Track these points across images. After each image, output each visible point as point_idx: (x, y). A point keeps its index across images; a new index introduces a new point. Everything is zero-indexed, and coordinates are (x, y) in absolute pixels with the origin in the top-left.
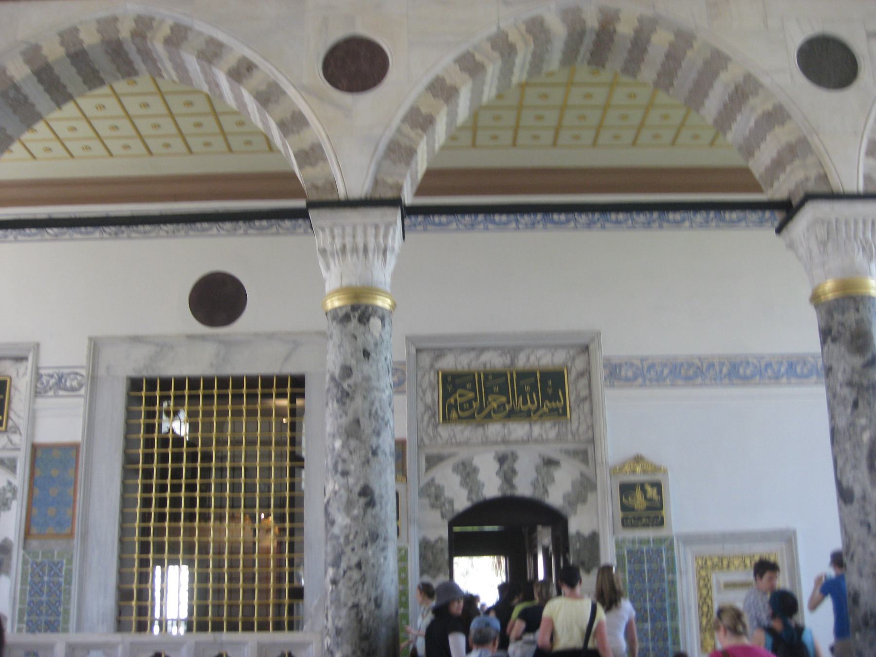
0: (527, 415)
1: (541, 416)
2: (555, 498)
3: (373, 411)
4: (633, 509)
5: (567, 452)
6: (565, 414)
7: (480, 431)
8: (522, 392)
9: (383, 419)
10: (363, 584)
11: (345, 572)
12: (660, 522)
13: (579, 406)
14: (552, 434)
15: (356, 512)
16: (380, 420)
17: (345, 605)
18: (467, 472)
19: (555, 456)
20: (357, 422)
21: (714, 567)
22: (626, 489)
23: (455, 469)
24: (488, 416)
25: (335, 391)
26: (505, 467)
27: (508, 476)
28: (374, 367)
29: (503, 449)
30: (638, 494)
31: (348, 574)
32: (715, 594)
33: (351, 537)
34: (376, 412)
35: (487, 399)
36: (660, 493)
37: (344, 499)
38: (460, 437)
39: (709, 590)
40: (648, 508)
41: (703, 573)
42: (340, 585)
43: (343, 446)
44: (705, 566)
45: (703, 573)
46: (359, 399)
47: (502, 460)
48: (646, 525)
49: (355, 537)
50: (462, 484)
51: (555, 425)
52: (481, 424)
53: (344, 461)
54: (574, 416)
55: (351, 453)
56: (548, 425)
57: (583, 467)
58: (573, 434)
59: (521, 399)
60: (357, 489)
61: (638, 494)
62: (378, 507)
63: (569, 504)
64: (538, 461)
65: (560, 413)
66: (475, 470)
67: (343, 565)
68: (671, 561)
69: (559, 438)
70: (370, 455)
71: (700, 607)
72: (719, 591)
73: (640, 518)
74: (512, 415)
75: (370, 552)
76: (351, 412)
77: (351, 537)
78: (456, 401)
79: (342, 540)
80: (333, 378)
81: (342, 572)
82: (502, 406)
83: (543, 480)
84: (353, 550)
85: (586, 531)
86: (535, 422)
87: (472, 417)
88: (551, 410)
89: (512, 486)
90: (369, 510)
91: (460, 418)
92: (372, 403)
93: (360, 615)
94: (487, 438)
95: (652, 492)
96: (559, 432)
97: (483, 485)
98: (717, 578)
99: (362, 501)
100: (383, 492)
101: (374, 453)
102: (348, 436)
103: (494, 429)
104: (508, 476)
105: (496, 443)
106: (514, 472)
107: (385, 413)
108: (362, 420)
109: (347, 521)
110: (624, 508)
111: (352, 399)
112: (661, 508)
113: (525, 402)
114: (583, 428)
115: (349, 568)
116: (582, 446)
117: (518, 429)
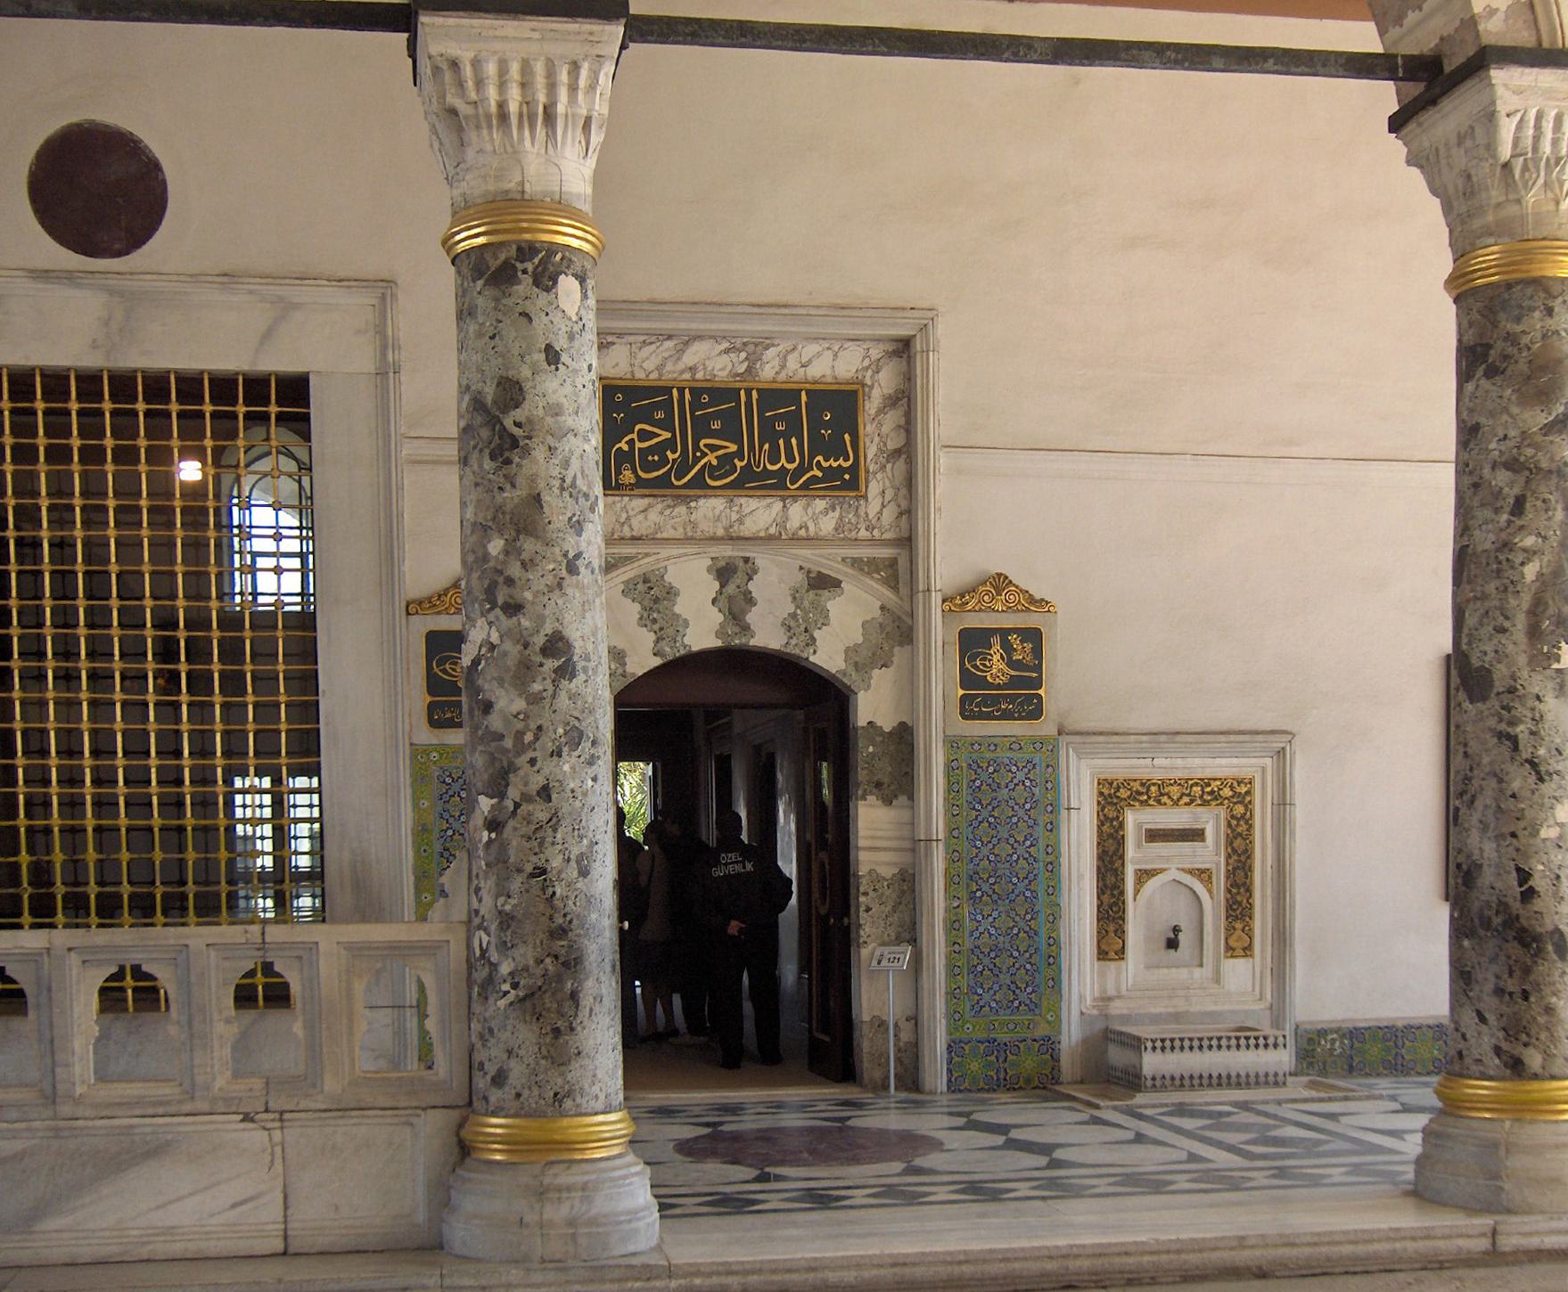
0: (776, 484)
1: (805, 487)
2: (828, 656)
3: (568, 481)
4: (982, 683)
5: (856, 562)
6: (853, 485)
7: (682, 509)
8: (769, 434)
9: (586, 496)
10: (555, 830)
11: (517, 805)
12: (1034, 710)
13: (883, 468)
14: (827, 525)
15: (537, 687)
16: (582, 500)
17: (519, 871)
18: (654, 597)
19: (834, 569)
20: (537, 498)
21: (1135, 796)
22: (972, 642)
23: (629, 590)
24: (698, 483)
25: (485, 433)
26: (731, 589)
27: (736, 607)
28: (568, 389)
29: (727, 551)
30: (996, 651)
31: (525, 808)
32: (1131, 851)
33: (529, 737)
34: (573, 485)
35: (696, 447)
36: (1038, 652)
37: (511, 662)
38: (640, 525)
39: (1121, 842)
40: (1014, 682)
42: (508, 830)
43: (507, 553)
46: (539, 453)
47: (724, 573)
48: (1006, 716)
49: (537, 739)
50: (642, 621)
51: (834, 509)
52: (686, 500)
53: (510, 582)
54: (874, 489)
55: (524, 565)
56: (820, 504)
57: (888, 593)
59: (766, 446)
60: (539, 640)
61: (996, 651)
62: (582, 677)
63: (856, 664)
64: (801, 577)
65: (848, 482)
66: (671, 593)
67: (513, 793)
69: (842, 536)
70: (564, 573)
72: (1139, 846)
73: (995, 700)
74: (750, 481)
75: (566, 768)
76: (520, 481)
77: (529, 737)
78: (631, 443)
79: (508, 743)
80: (478, 404)
81: (509, 804)
82: (726, 460)
84: (533, 762)
85: (887, 724)
86: (795, 498)
87: (663, 482)
88: (831, 474)
89: (746, 628)
90: (564, 683)
91: (641, 483)
92: (566, 464)
93: (550, 890)
94: (695, 525)
95: (1022, 651)
96: (841, 518)
97: (686, 623)
98: (1134, 820)
99: (551, 664)
100: (590, 647)
101: (572, 569)
102: (518, 532)
103: (710, 510)
104: (736, 607)
105: (714, 539)
106: (751, 601)
107: (590, 487)
108: (546, 498)
109: (519, 704)
110: (967, 679)
111: (527, 452)
113: (774, 459)
114: (889, 515)
115: (527, 798)
116: (886, 553)
117: (760, 513)
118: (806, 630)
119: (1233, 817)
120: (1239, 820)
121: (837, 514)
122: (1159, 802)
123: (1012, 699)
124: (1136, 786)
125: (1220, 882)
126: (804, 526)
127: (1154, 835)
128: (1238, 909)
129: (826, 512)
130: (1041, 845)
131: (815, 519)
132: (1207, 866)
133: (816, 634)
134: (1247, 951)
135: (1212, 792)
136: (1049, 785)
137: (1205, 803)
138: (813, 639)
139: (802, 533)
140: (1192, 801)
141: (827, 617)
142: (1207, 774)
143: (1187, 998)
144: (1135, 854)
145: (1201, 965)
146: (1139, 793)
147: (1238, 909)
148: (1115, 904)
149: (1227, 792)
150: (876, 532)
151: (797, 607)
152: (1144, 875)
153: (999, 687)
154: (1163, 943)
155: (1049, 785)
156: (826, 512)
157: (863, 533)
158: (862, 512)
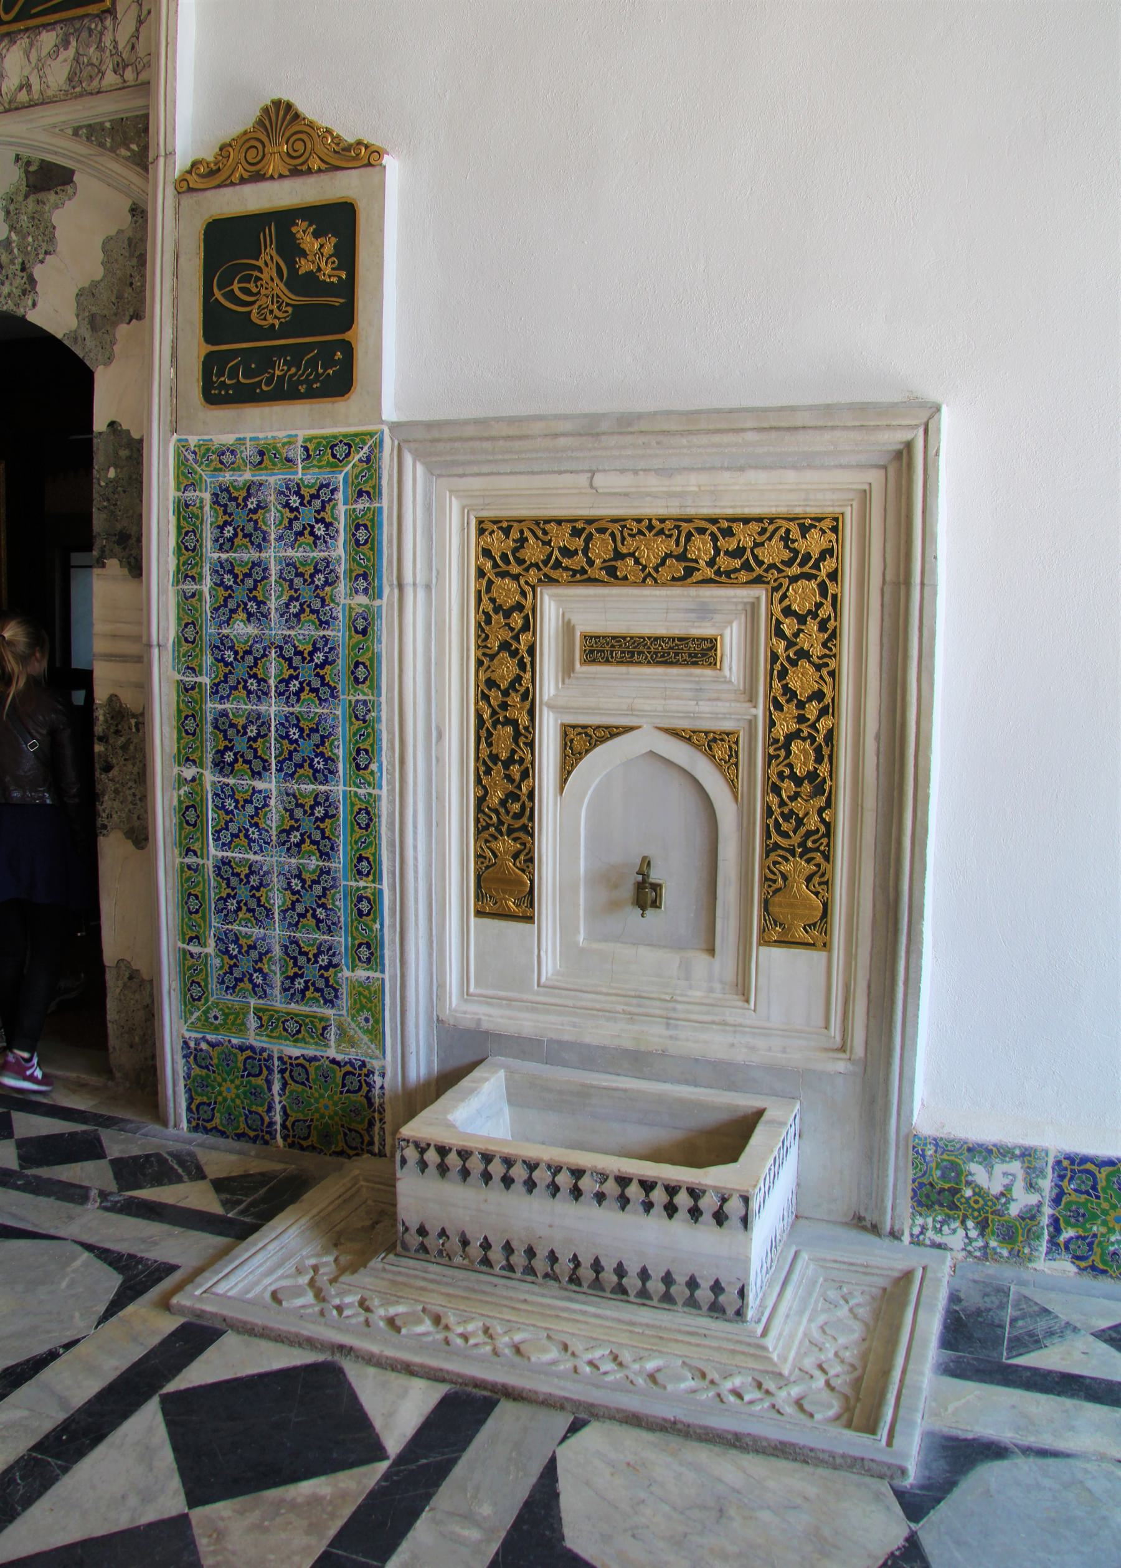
14: (58, 74)
19: (63, 150)
22: (229, 245)
30: (269, 258)
32: (548, 682)
36: (347, 255)
41: (507, 591)
44: (520, 558)
45: (507, 591)
58: (120, 68)
61: (269, 258)
68: (365, 534)
71: (484, 732)
72: (568, 669)
83: (23, 250)
96: (76, 60)
98: (555, 610)
112: (346, 317)
118: (23, 269)
119: (788, 612)
120: (802, 619)
121: (71, 52)
122: (612, 571)
123: (297, 352)
124: (562, 538)
125: (755, 765)
126: (26, 85)
127: (605, 650)
128: (795, 837)
129: (55, 53)
130: (342, 664)
131: (40, 68)
132: (727, 725)
133: (38, 271)
134: (816, 932)
135: (739, 552)
136: (362, 535)
137: (722, 578)
138: (32, 281)
139: (23, 96)
140: (689, 572)
141: (52, 240)
142: (726, 508)
143: (668, 1021)
144: (559, 694)
145: (711, 951)
146: (566, 552)
147: (795, 837)
148: (513, 796)
149: (774, 552)
150: (129, 74)
151: (12, 228)
152: (580, 741)
153: (270, 332)
154: (627, 892)
155: (362, 535)
156: (55, 53)
157: (111, 78)
158: (107, 40)
